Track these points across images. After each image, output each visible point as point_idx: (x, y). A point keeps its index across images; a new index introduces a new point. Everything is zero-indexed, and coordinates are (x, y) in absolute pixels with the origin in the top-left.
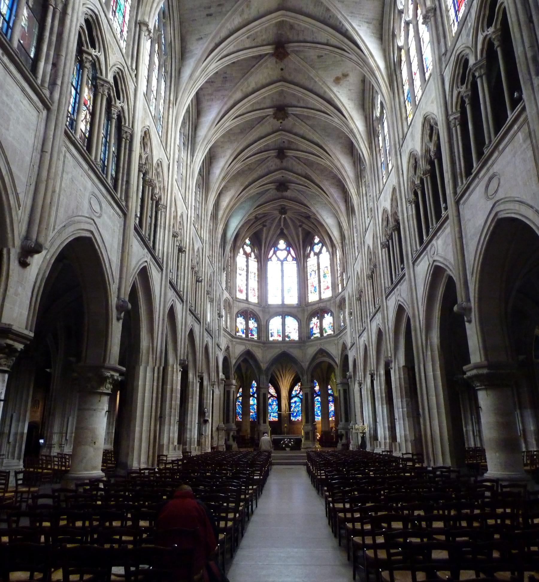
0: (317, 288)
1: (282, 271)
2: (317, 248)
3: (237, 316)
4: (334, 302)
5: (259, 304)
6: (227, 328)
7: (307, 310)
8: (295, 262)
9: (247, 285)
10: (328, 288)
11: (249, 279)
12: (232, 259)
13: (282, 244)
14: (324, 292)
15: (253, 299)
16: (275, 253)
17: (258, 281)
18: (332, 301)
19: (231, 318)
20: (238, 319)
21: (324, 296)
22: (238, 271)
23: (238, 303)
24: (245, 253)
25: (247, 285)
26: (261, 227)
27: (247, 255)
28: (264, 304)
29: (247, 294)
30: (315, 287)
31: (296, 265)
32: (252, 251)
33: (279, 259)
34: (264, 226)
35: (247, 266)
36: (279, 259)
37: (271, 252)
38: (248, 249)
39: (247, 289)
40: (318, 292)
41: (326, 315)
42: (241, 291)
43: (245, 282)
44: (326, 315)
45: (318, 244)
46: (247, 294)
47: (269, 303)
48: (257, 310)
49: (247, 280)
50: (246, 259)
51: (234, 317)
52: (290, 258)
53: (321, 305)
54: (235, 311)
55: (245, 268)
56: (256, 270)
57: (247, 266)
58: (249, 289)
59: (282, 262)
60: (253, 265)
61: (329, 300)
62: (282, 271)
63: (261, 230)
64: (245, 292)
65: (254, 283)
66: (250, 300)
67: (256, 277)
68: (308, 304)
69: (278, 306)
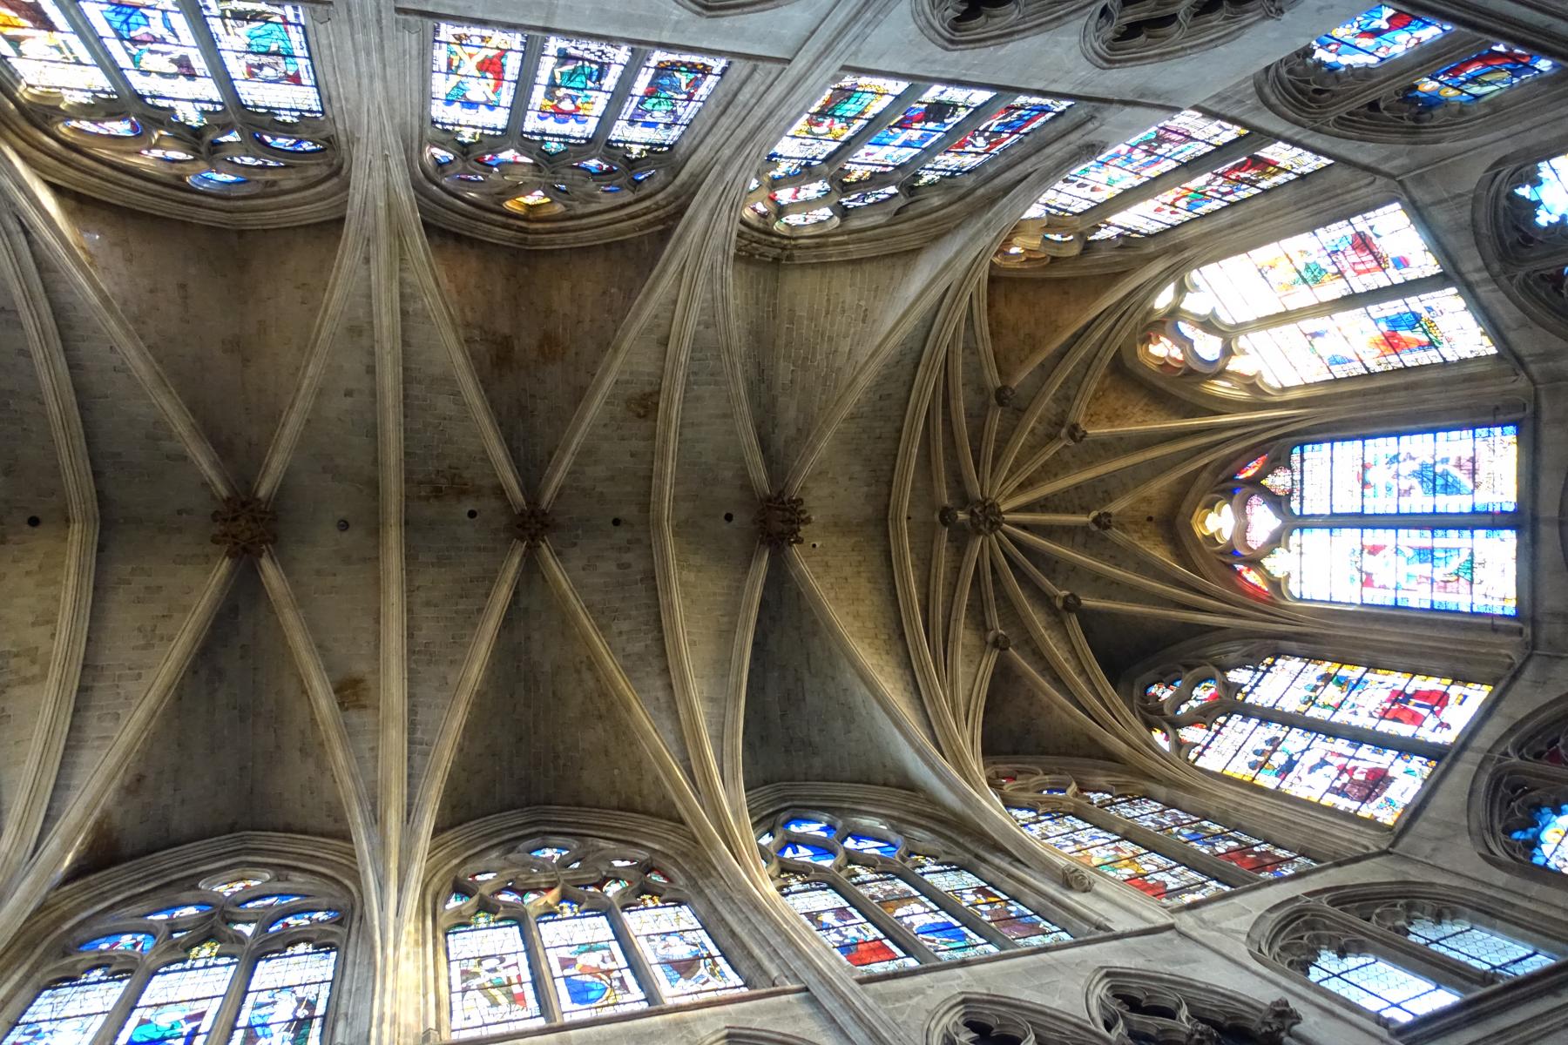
0: (1393, 307)
1: (1336, 521)
2: (1208, 347)
3: (1523, 859)
4: (1420, 180)
5: (1504, 681)
6: (1486, 978)
7: (1547, 356)
8: (1297, 450)
9: (1358, 737)
10: (1362, 243)
11: (1342, 717)
12: (1179, 795)
13: (1219, 522)
14: (1401, 263)
15: (1465, 704)
16: (1254, 562)
17: (1372, 666)
18: (1419, 194)
19: (1490, 913)
20: (1547, 849)
21: (1425, 264)
22: (1267, 780)
23: (1421, 826)
24: (1204, 717)
25: (1358, 737)
26: (1074, 618)
27: (1230, 705)
28: (1509, 650)
29: (1407, 748)
30: (1394, 323)
31: (1308, 448)
32: (1212, 678)
33: (1277, 540)
34: (1072, 605)
35: (1267, 716)
36: (1277, 540)
37: (1252, 577)
38: (1203, 694)
39: (1382, 742)
40: (1415, 303)
41: (1543, 219)
42: (1378, 781)
43: (1341, 745)
44: (1543, 219)
45: (1184, 342)
46: (1407, 748)
47: (1510, 609)
48: (1525, 701)
49: (1331, 731)
50: (1236, 718)
51: (1500, 877)
52: (1278, 481)
53: (1471, 264)
54: (1461, 861)
55: (1274, 730)
56: (1311, 666)
57: (1267, 716)
58: (1387, 727)
59: (1294, 521)
60: (1284, 683)
61: (1419, 213)
62: (1336, 521)
63: (1089, 619)
64: (1385, 759)
65: (1369, 696)
66: (1448, 737)
67: (1346, 671)
68: (1509, 357)
69: (1529, 557)
